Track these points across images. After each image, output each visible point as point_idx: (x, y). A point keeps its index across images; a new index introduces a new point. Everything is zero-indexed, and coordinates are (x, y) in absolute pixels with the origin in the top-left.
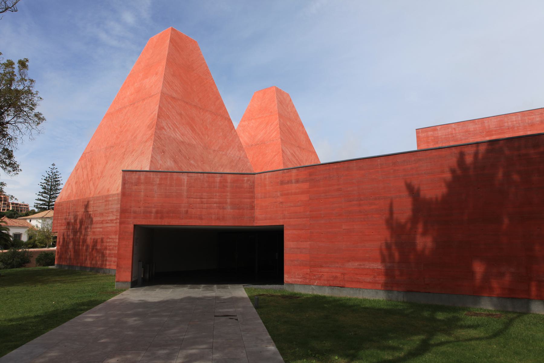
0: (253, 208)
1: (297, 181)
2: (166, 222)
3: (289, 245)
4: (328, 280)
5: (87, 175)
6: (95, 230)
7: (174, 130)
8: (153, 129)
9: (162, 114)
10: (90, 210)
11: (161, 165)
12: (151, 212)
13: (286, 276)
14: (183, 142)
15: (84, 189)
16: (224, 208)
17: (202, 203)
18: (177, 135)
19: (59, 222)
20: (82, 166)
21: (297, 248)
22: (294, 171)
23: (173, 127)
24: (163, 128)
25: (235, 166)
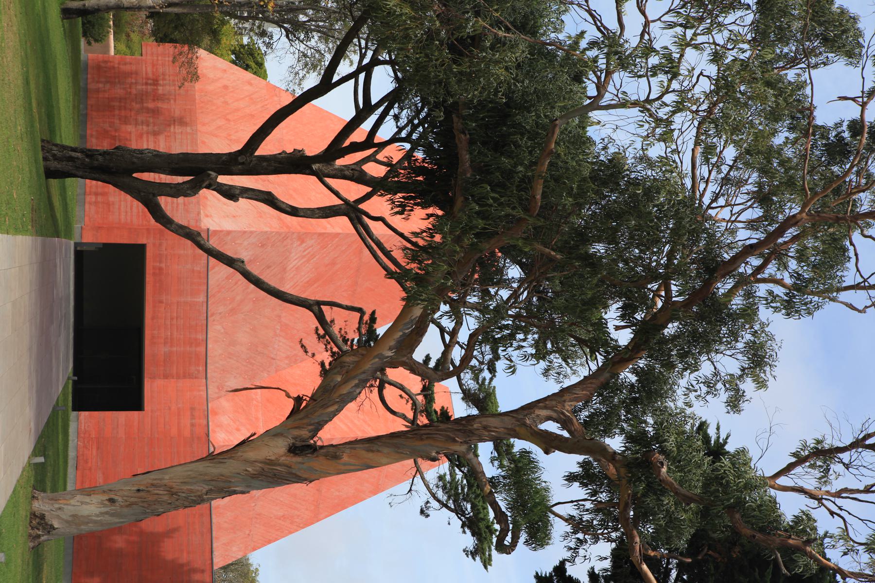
0: (166, 377)
1: (192, 425)
2: (149, 279)
3: (122, 416)
4: (83, 455)
5: (237, 110)
6: (145, 139)
7: (304, 256)
8: (299, 228)
9: (326, 239)
10: (176, 127)
11: (241, 244)
12: (160, 262)
13: (87, 413)
14: (284, 270)
15: (214, 108)
16: (165, 343)
17: (172, 319)
18: (296, 261)
19: (160, 58)
20: (256, 92)
21: (118, 425)
22: (205, 422)
23: (308, 254)
24: (303, 242)
25: (257, 351)
